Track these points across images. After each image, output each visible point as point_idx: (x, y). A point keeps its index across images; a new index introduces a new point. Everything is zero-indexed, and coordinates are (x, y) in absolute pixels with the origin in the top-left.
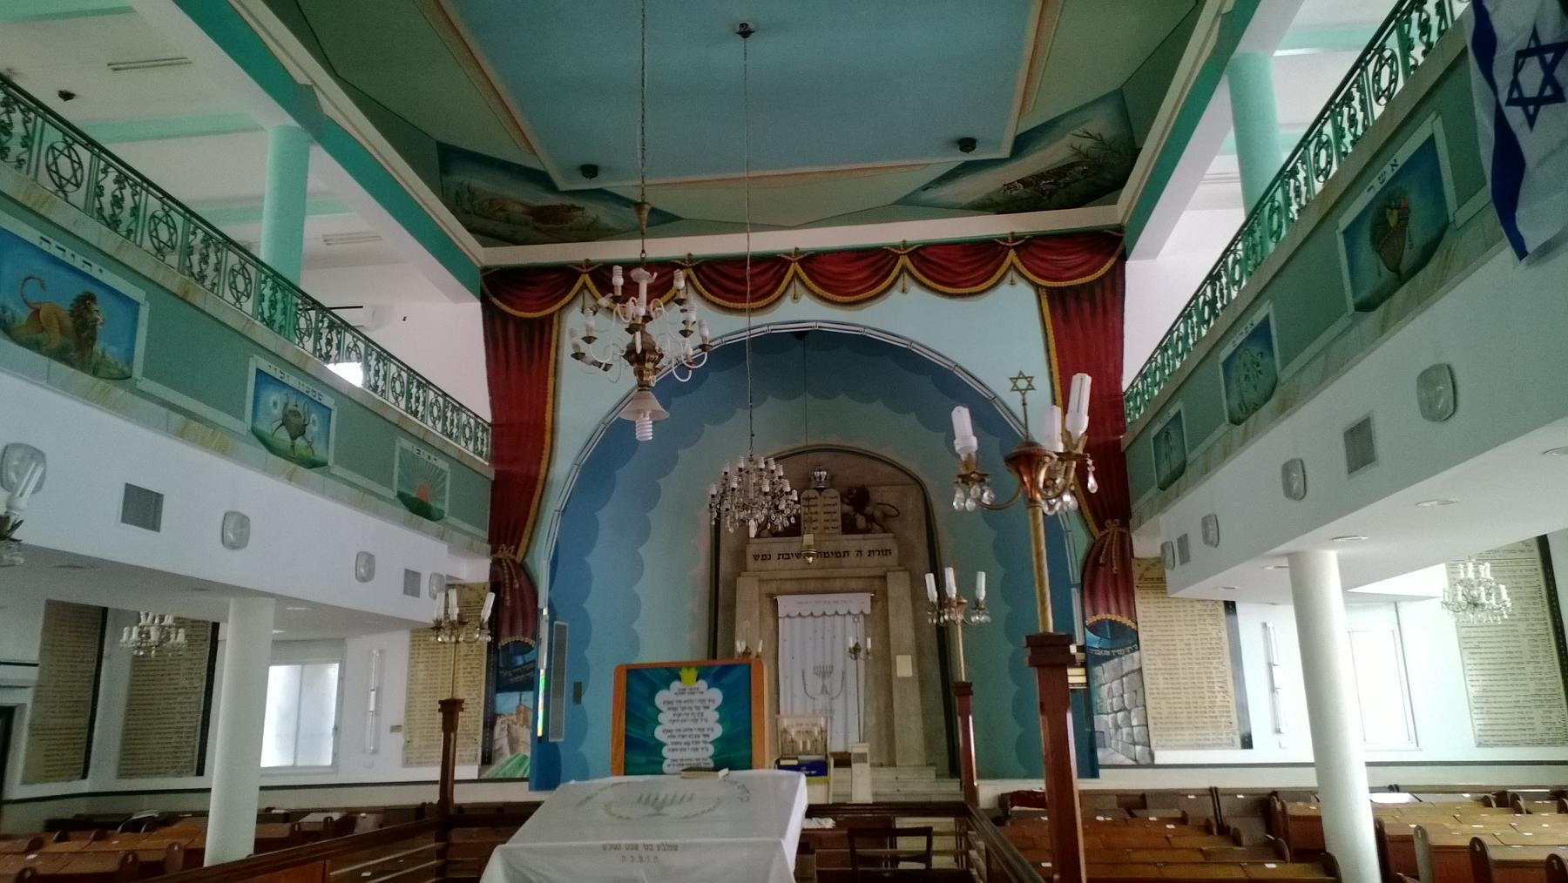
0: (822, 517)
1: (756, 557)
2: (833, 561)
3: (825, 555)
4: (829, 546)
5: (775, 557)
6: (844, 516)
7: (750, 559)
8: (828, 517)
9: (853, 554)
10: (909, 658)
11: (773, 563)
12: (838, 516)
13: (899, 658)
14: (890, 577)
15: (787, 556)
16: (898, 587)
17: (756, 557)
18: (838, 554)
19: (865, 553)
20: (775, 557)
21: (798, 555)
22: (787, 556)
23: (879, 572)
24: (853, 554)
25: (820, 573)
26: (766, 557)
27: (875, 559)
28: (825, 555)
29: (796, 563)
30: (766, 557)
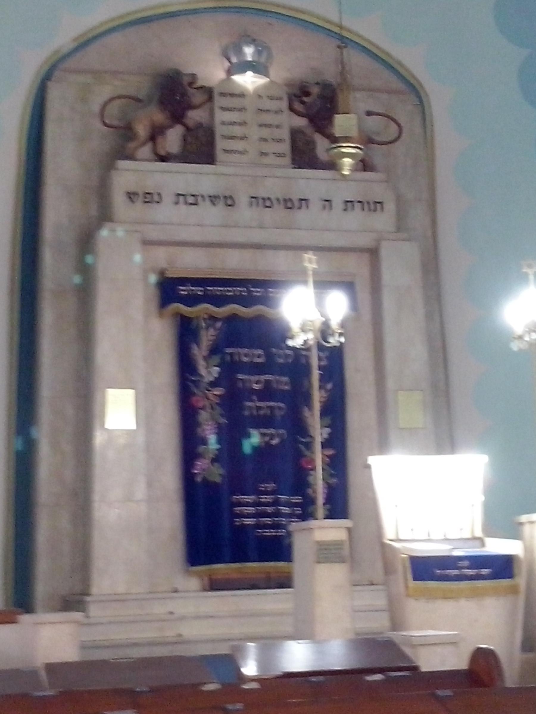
0: (255, 133)
1: (131, 196)
2: (277, 213)
3: (266, 203)
4: (272, 188)
5: (168, 199)
6: (295, 133)
7: (119, 200)
8: (265, 132)
9: (316, 205)
10: (417, 396)
11: (166, 211)
12: (285, 134)
13: (402, 396)
14: (384, 252)
15: (193, 200)
16: (400, 269)
17: (131, 196)
18: (288, 204)
19: (338, 204)
20: (168, 199)
21: (213, 199)
22: (193, 200)
23: (364, 240)
24: (316, 205)
25: (258, 236)
26: (150, 198)
27: (355, 219)
28: (266, 203)
29: (212, 214)
30: (150, 198)
